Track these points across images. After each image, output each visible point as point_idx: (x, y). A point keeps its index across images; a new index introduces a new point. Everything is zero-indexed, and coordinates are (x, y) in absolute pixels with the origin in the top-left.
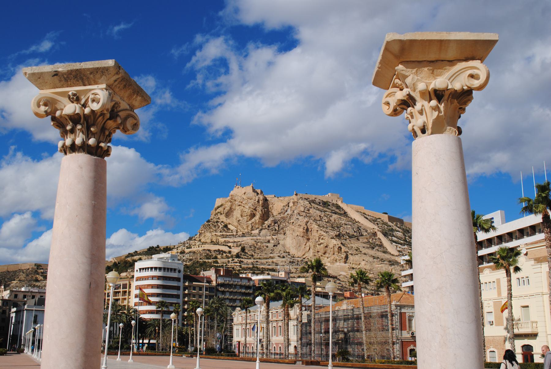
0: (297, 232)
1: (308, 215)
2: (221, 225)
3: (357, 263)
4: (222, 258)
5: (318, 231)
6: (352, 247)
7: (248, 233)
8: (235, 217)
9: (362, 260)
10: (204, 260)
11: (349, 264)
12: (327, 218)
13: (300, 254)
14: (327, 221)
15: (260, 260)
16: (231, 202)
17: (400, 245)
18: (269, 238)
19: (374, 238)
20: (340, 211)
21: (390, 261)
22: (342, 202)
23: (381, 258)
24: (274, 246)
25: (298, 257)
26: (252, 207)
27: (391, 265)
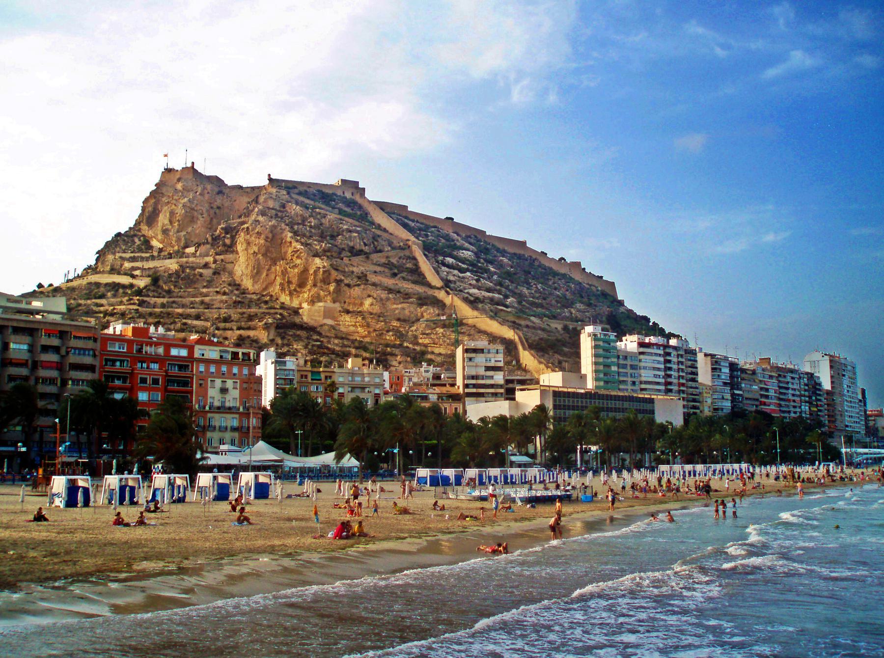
0: (254, 247)
1: (280, 214)
2: (140, 240)
3: (356, 302)
7: (178, 251)
8: (160, 224)
9: (366, 296)
14: (313, 224)
15: (180, 299)
17: (456, 272)
18: (210, 259)
20: (352, 210)
24: (214, 273)
26: (188, 205)
27: (421, 305)
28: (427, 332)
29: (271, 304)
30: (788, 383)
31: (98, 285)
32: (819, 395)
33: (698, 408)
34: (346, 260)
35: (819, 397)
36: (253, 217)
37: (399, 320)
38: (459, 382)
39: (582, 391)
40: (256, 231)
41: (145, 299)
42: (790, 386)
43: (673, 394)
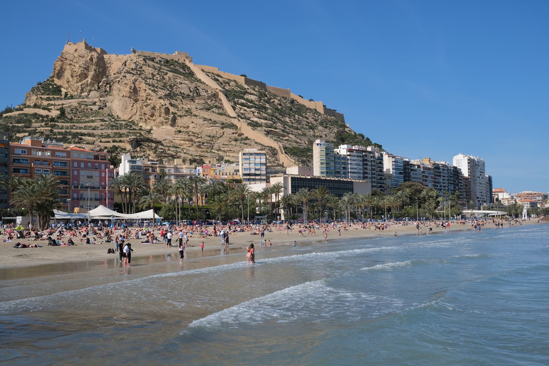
0: (123, 92)
3: (185, 126)
4: (36, 122)
5: (145, 90)
6: (183, 108)
8: (65, 78)
9: (191, 122)
10: (14, 125)
11: (177, 127)
12: (160, 76)
13: (126, 117)
14: (159, 79)
15: (78, 124)
16: (62, 61)
18: (97, 100)
19: (214, 99)
21: (223, 124)
22: (190, 61)
23: (214, 120)
24: (99, 109)
25: (124, 120)
26: (82, 66)
28: (226, 144)
29: (133, 127)
30: (440, 172)
31: (26, 115)
32: (461, 180)
33: (383, 187)
34: (179, 101)
35: (460, 181)
36: (123, 74)
37: (209, 136)
38: (240, 173)
39: (309, 177)
40: (124, 83)
41: (56, 123)
42: (442, 174)
43: (368, 179)
